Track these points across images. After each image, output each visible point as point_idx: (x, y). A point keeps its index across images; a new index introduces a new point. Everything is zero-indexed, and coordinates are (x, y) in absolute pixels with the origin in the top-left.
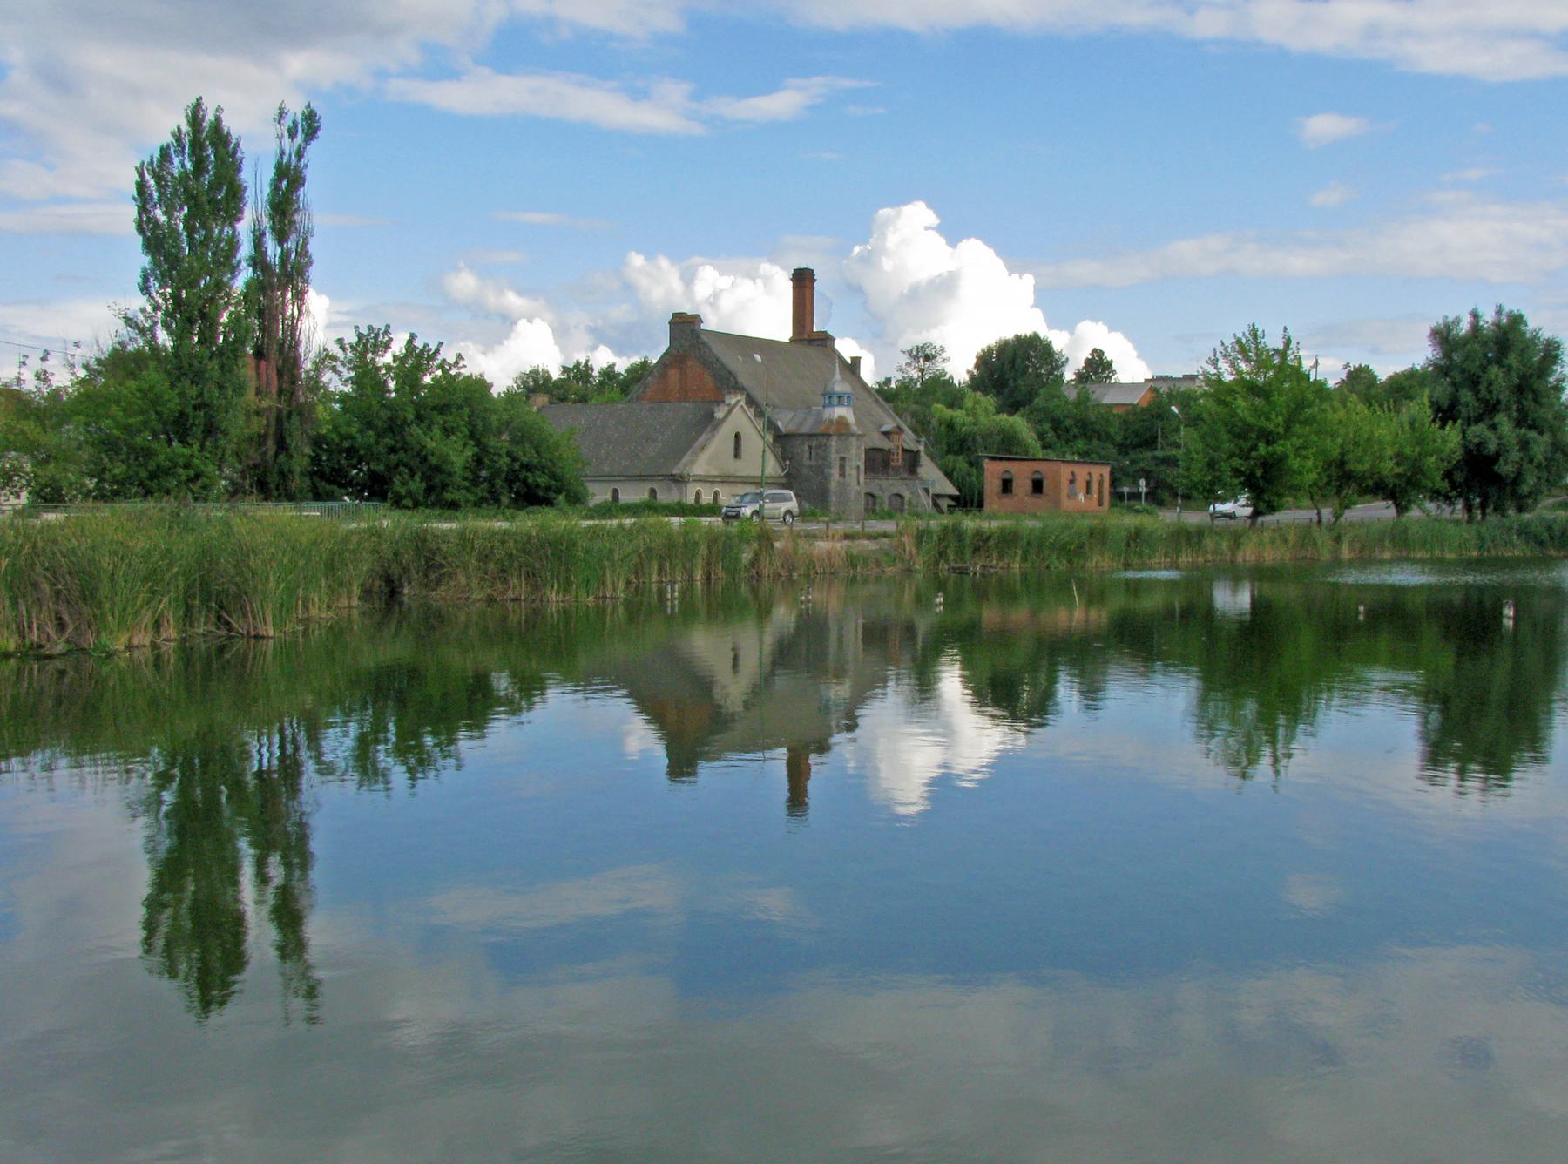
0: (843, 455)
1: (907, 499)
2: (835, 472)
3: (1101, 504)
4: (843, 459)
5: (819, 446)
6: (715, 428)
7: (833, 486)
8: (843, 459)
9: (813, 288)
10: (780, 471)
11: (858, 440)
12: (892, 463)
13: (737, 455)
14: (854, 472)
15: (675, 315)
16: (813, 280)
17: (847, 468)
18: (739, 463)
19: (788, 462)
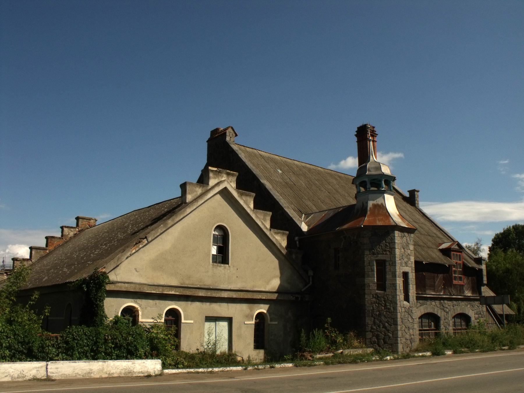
0: (380, 257)
1: (473, 319)
11: (402, 237)
12: (455, 282)
14: (400, 281)
16: (374, 135)
17: (389, 276)
18: (221, 269)
19: (311, 273)
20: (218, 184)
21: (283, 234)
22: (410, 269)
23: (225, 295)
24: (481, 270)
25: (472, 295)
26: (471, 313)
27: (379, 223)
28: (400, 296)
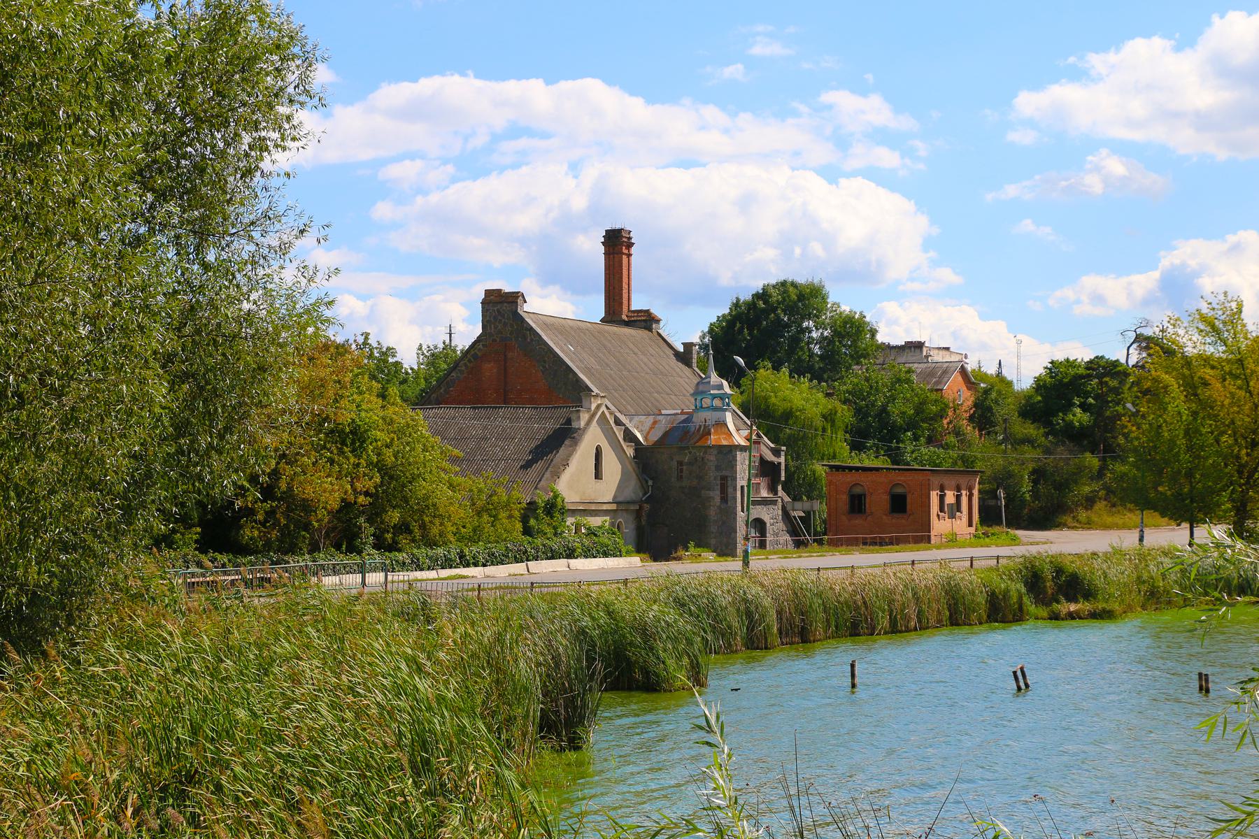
0: (724, 473)
1: (768, 525)
2: (716, 495)
3: (970, 525)
4: (724, 478)
5: (690, 464)
6: (576, 443)
7: (712, 513)
8: (724, 478)
9: (629, 255)
10: (641, 495)
13: (598, 475)
15: (488, 292)
16: (630, 245)
17: (730, 490)
19: (650, 483)
20: (598, 407)
21: (631, 446)
22: (744, 483)
23: (605, 507)
24: (780, 464)
25: (768, 494)
26: (766, 518)
27: (725, 443)
28: (739, 508)
